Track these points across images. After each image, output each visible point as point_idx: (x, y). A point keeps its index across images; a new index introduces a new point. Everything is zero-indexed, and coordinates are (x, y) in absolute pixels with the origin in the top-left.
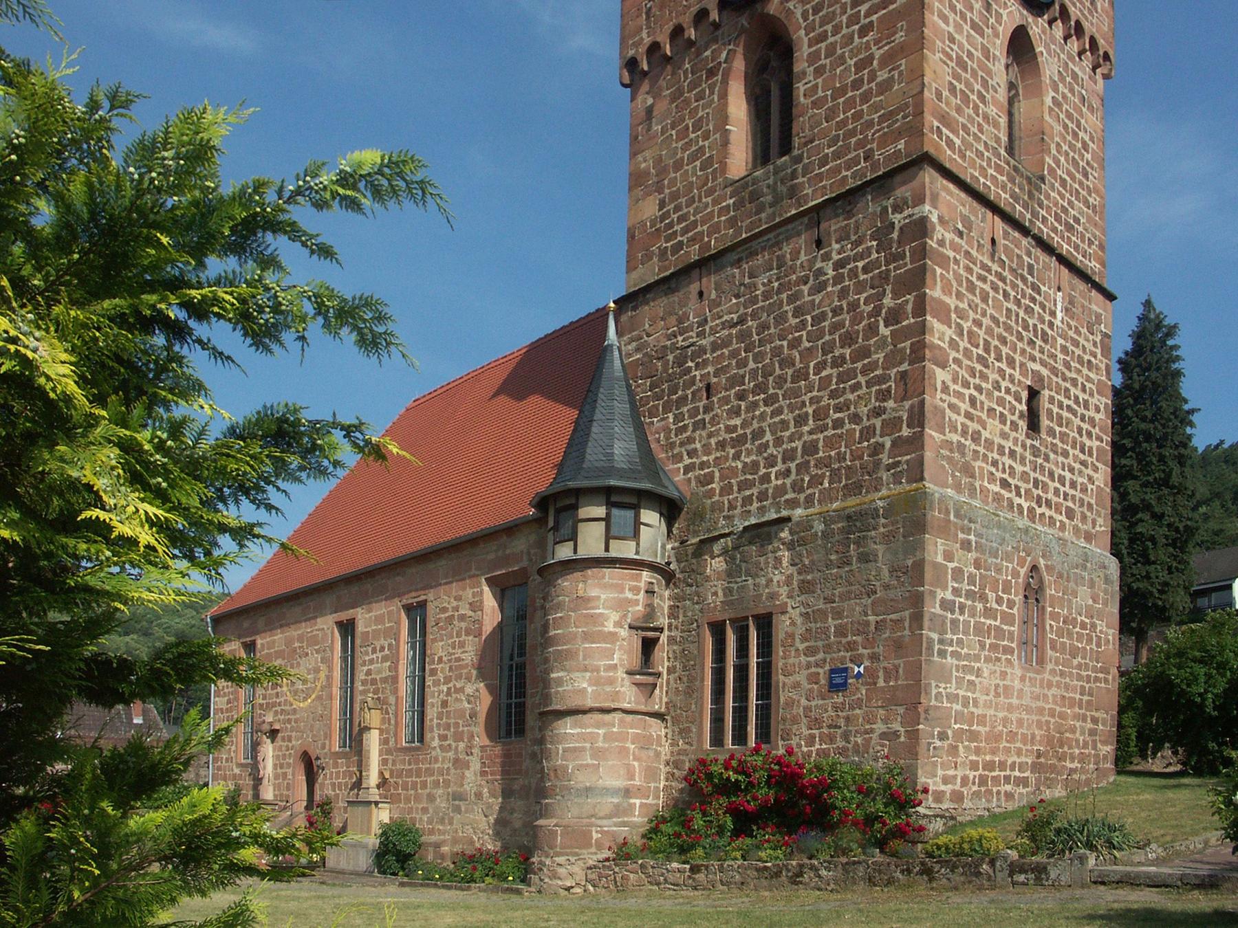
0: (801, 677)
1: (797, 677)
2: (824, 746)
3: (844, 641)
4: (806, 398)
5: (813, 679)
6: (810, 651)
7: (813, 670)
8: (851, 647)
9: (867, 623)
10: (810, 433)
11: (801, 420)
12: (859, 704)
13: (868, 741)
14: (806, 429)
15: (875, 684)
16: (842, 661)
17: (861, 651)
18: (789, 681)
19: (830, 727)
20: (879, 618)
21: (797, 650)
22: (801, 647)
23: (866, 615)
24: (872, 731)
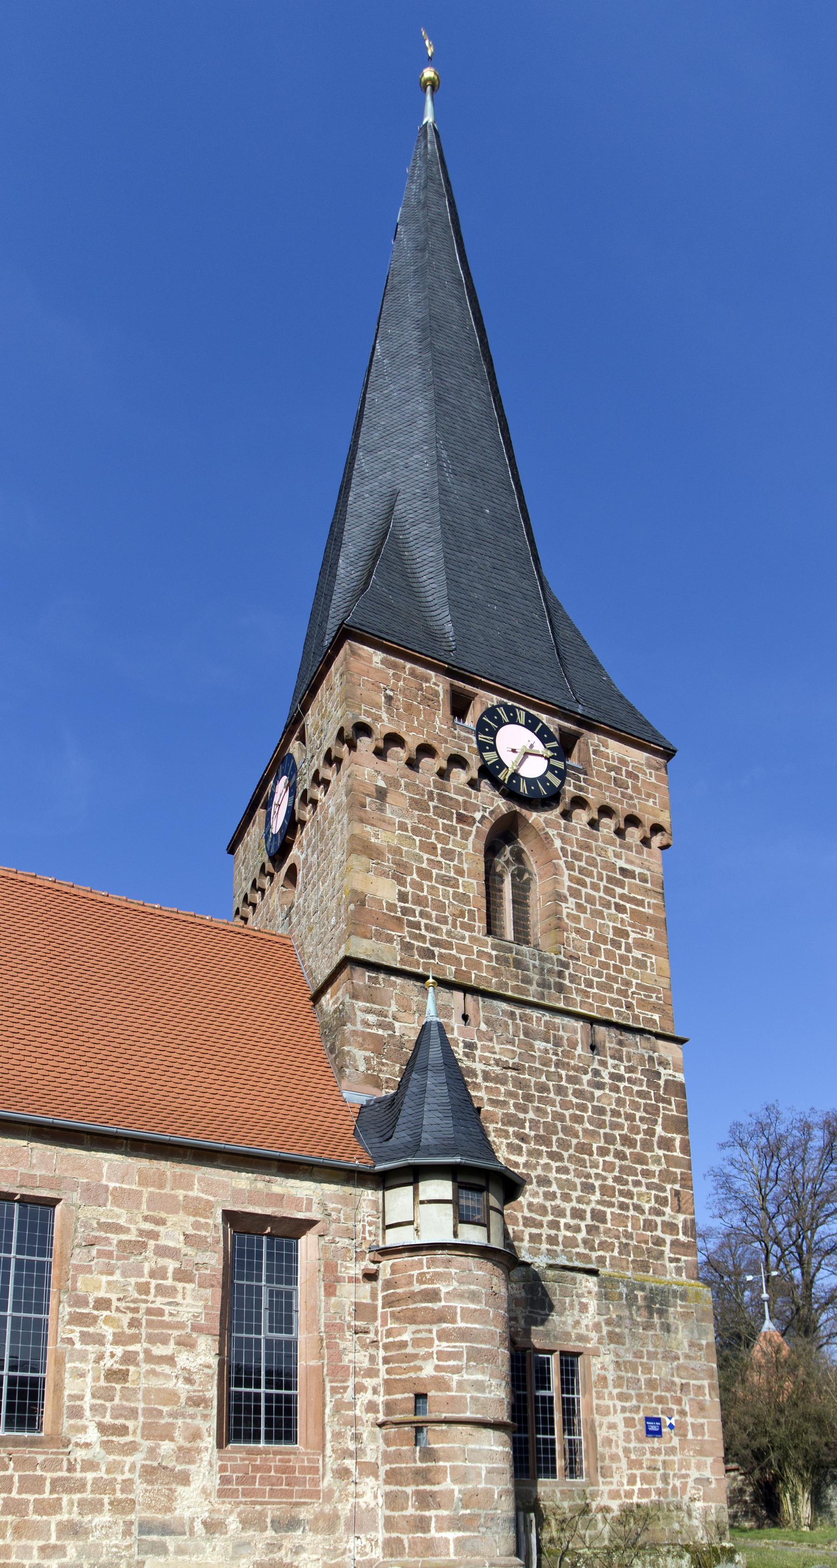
0: (618, 1419)
1: (611, 1419)
2: (645, 1486)
3: (655, 1394)
4: (593, 1171)
5: (629, 1422)
6: (622, 1397)
7: (628, 1415)
8: (660, 1400)
9: (673, 1383)
10: (598, 1202)
11: (588, 1188)
12: (672, 1451)
13: (684, 1485)
14: (593, 1198)
15: (686, 1435)
16: (655, 1410)
17: (670, 1406)
18: (606, 1420)
19: (649, 1468)
20: (684, 1381)
21: (610, 1393)
22: (615, 1391)
23: (673, 1375)
24: (687, 1476)
